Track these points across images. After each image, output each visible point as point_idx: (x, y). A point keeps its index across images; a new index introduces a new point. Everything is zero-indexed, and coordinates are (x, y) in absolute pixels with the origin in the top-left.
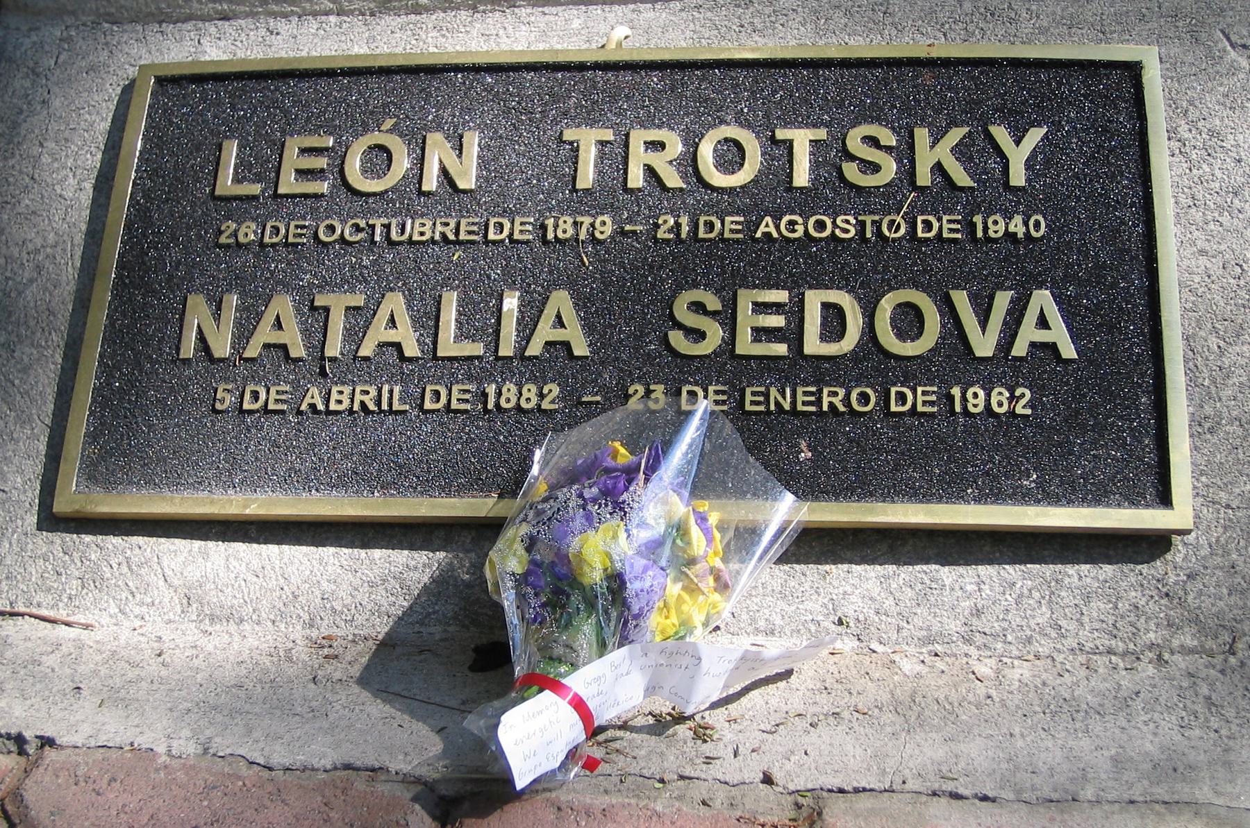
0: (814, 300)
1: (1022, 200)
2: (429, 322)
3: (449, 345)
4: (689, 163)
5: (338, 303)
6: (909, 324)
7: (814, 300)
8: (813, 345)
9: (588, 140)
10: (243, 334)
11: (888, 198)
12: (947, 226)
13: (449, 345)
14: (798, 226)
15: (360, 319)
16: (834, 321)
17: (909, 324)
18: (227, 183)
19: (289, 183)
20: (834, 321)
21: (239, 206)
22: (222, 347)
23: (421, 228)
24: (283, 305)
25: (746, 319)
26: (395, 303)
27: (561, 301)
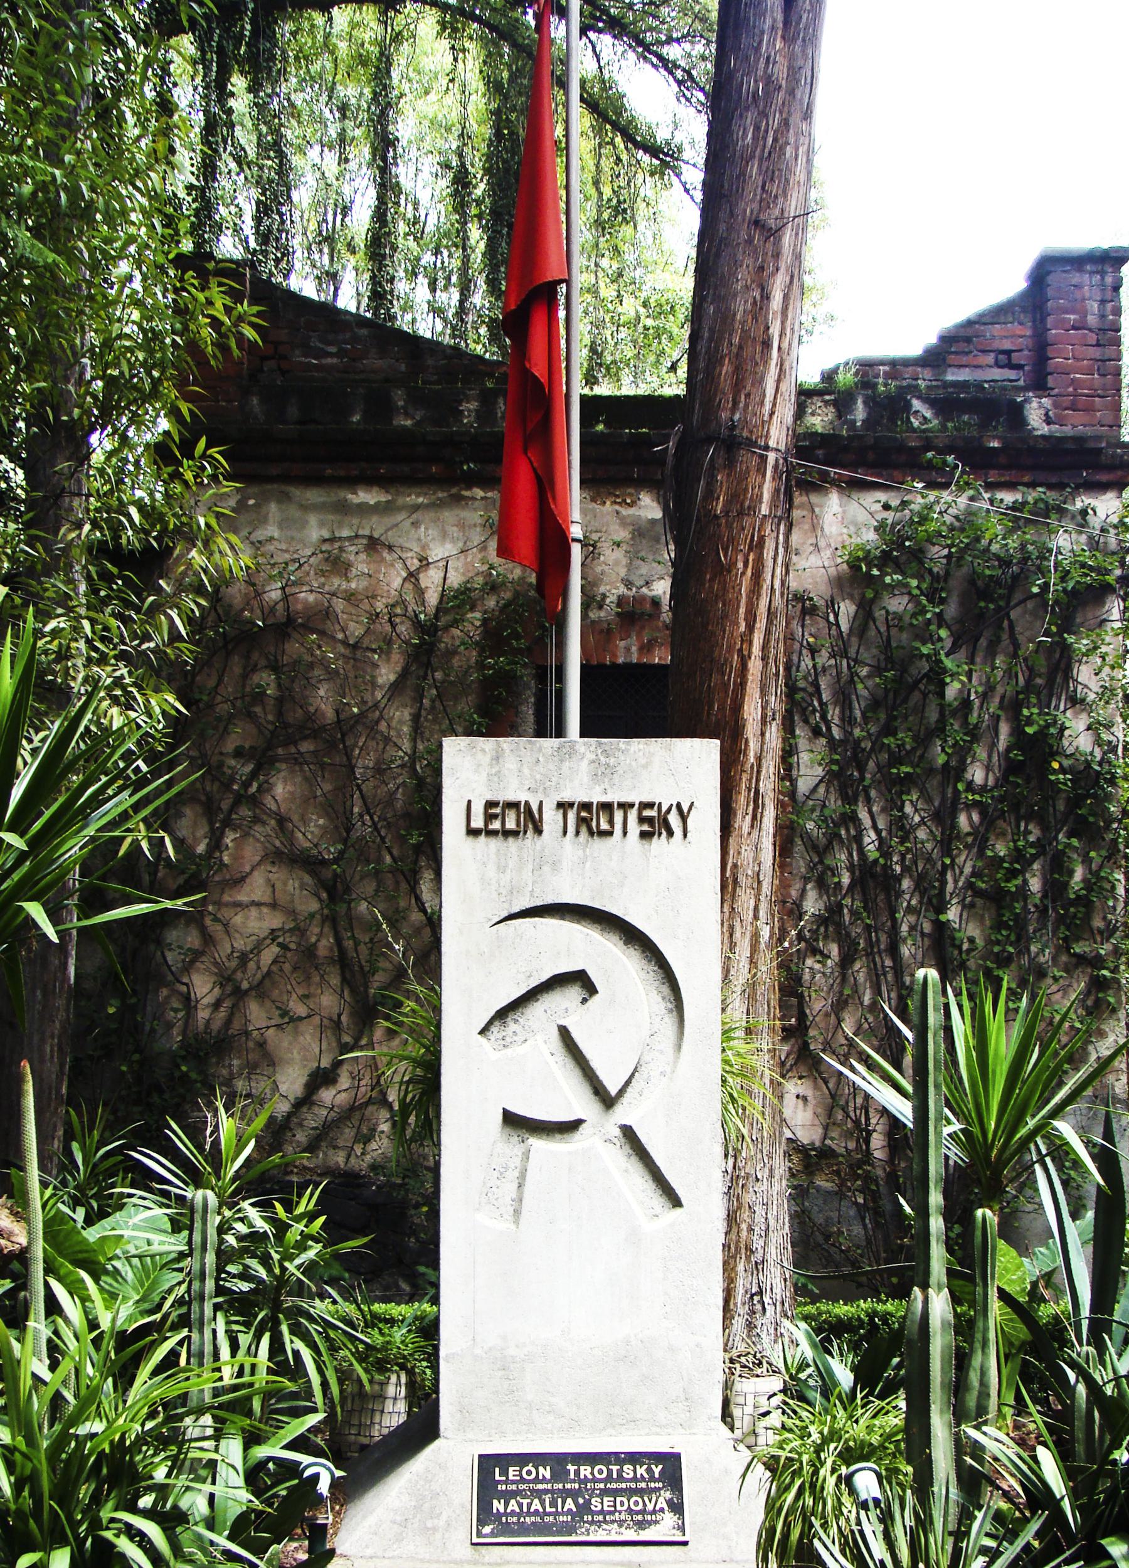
0: (618, 1499)
1: (655, 1480)
2: (542, 1503)
3: (548, 1509)
4: (592, 1473)
5: (525, 1502)
6: (636, 1503)
7: (618, 1499)
8: (619, 1508)
9: (571, 1468)
10: (506, 1508)
11: (630, 1480)
12: (644, 1485)
13: (548, 1509)
14: (614, 1486)
15: (529, 1505)
16: (622, 1503)
17: (636, 1503)
18: (497, 1477)
19: (511, 1477)
20: (622, 1503)
21: (499, 1482)
22: (502, 1510)
23: (540, 1486)
24: (513, 1502)
25: (606, 1504)
26: (536, 1501)
27: (569, 1500)
